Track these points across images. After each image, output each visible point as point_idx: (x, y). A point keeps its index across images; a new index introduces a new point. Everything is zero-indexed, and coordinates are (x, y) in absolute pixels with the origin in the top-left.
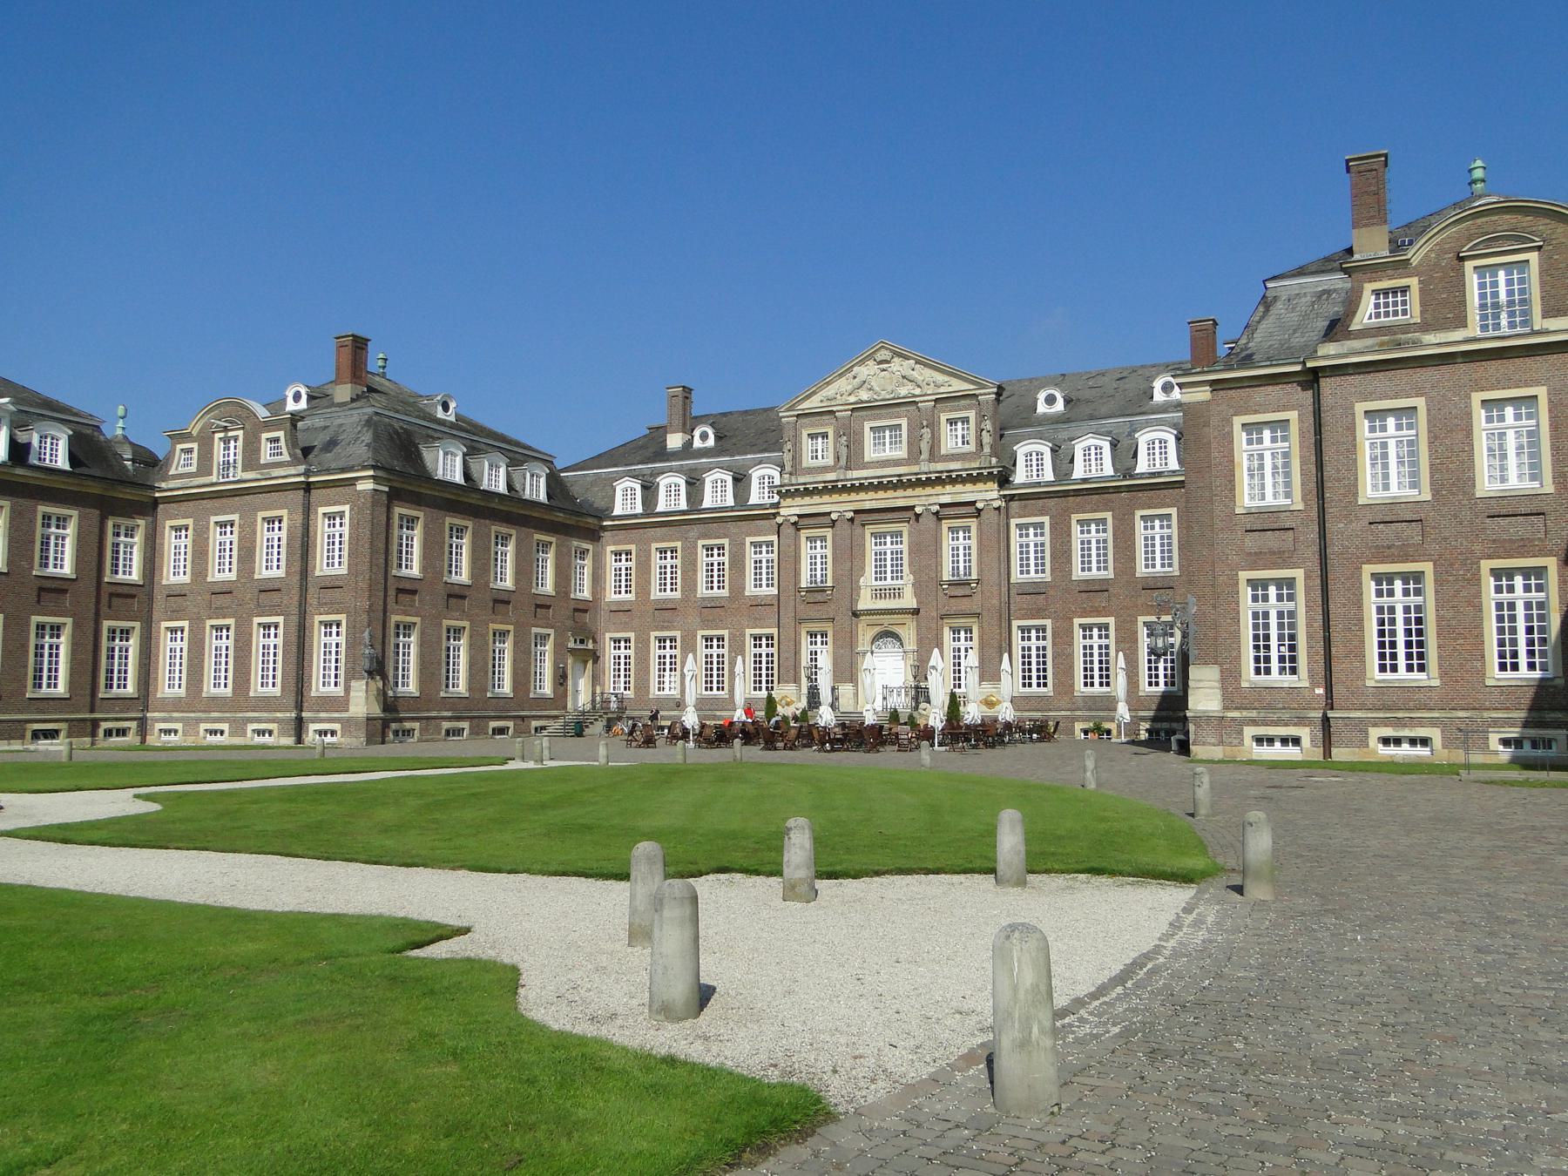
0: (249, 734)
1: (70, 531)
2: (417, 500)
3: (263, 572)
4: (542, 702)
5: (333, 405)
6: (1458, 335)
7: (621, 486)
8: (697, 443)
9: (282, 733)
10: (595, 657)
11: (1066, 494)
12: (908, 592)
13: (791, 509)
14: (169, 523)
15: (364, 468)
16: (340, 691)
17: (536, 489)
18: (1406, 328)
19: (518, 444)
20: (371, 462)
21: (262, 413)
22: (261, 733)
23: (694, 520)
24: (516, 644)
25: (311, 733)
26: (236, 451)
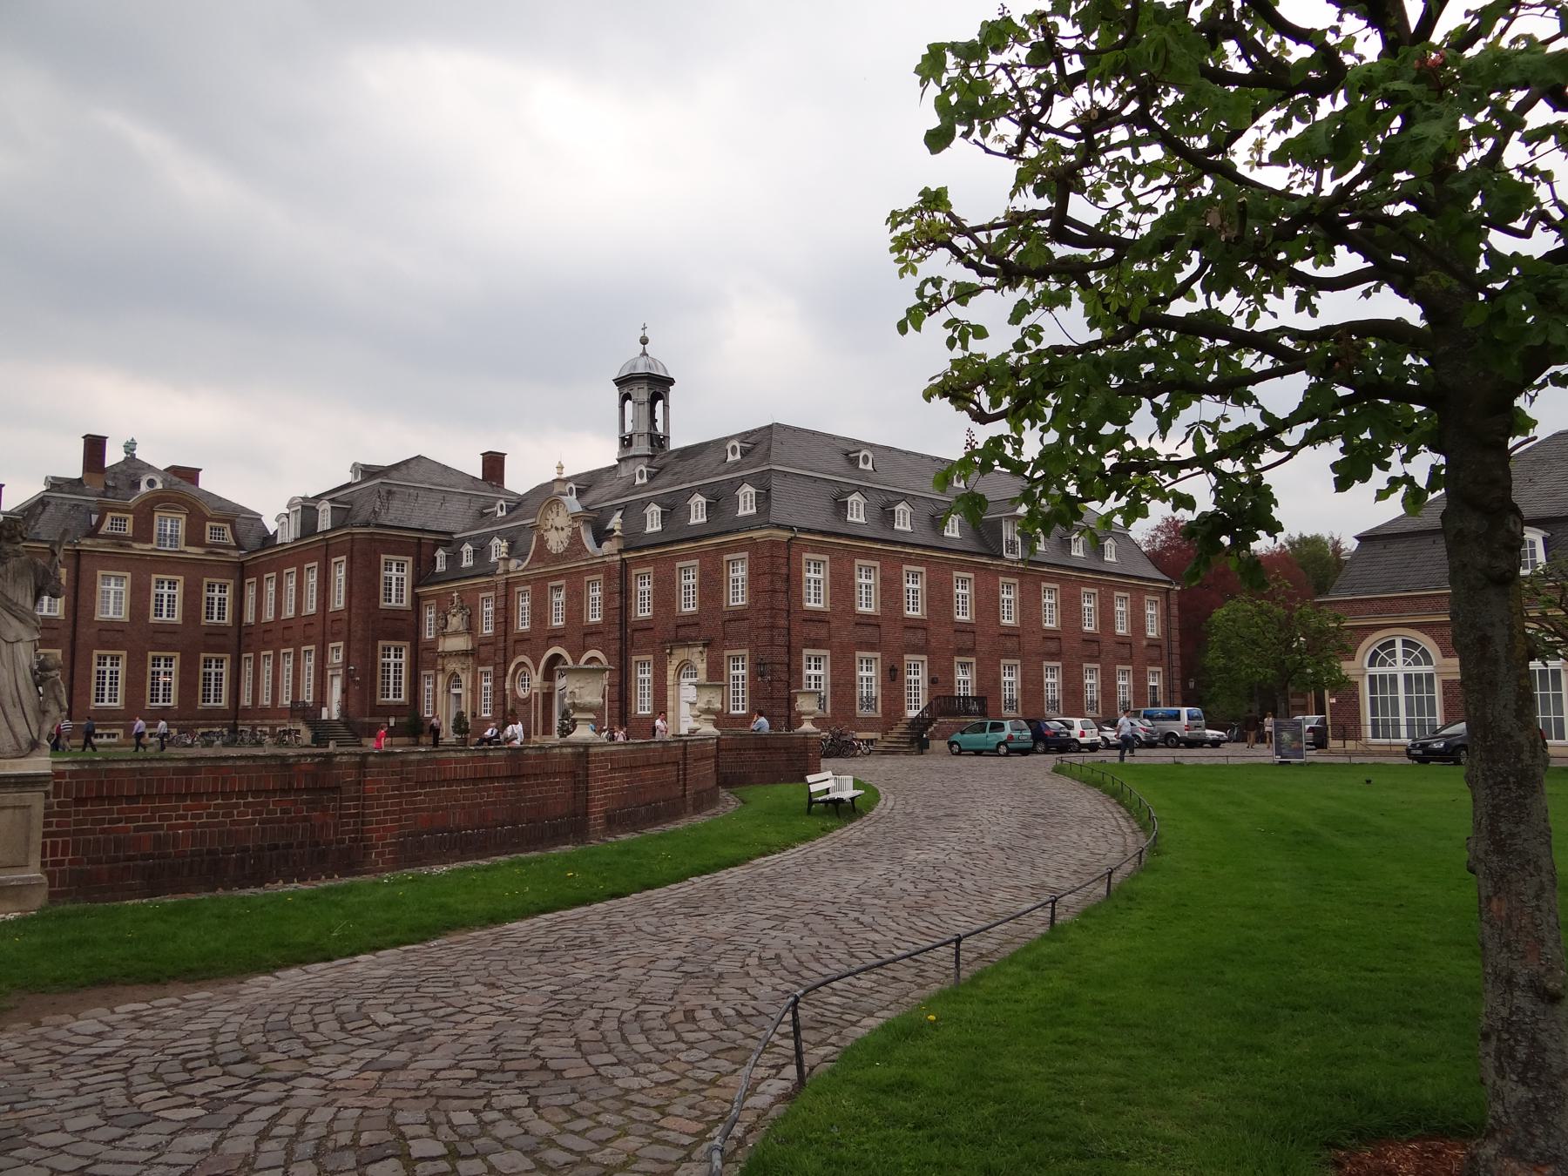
6: (149, 546)
18: (125, 538)
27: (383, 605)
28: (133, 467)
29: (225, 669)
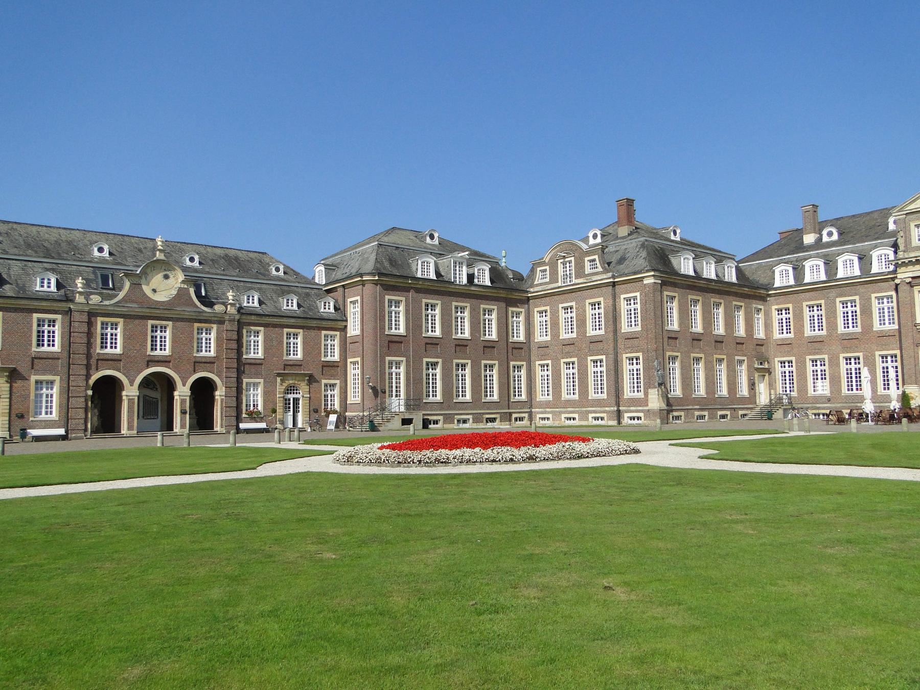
0: (590, 419)
1: (494, 316)
2: (674, 285)
3: (590, 332)
4: (743, 400)
5: (617, 238)
7: (777, 270)
8: (825, 239)
9: (609, 419)
10: (769, 371)
13: (905, 274)
14: (536, 310)
15: (648, 271)
16: (641, 395)
17: (731, 276)
19: (720, 252)
20: (648, 268)
21: (584, 247)
22: (596, 419)
23: (832, 285)
24: (728, 366)
25: (626, 418)
26: (572, 268)
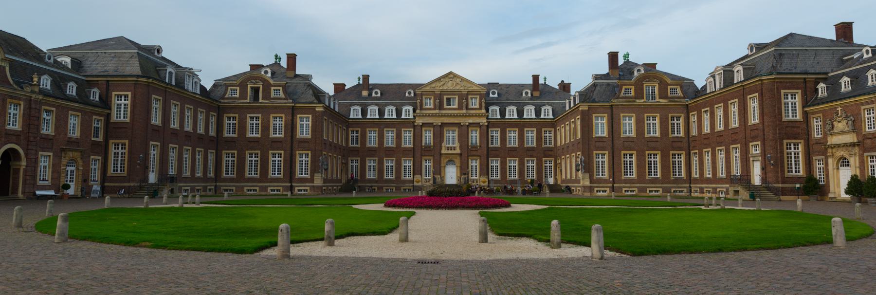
8: (374, 95)
9: (284, 190)
11: (505, 123)
12: (458, 148)
13: (419, 121)
16: (308, 176)
27: (784, 119)
28: (629, 66)
29: (683, 159)
